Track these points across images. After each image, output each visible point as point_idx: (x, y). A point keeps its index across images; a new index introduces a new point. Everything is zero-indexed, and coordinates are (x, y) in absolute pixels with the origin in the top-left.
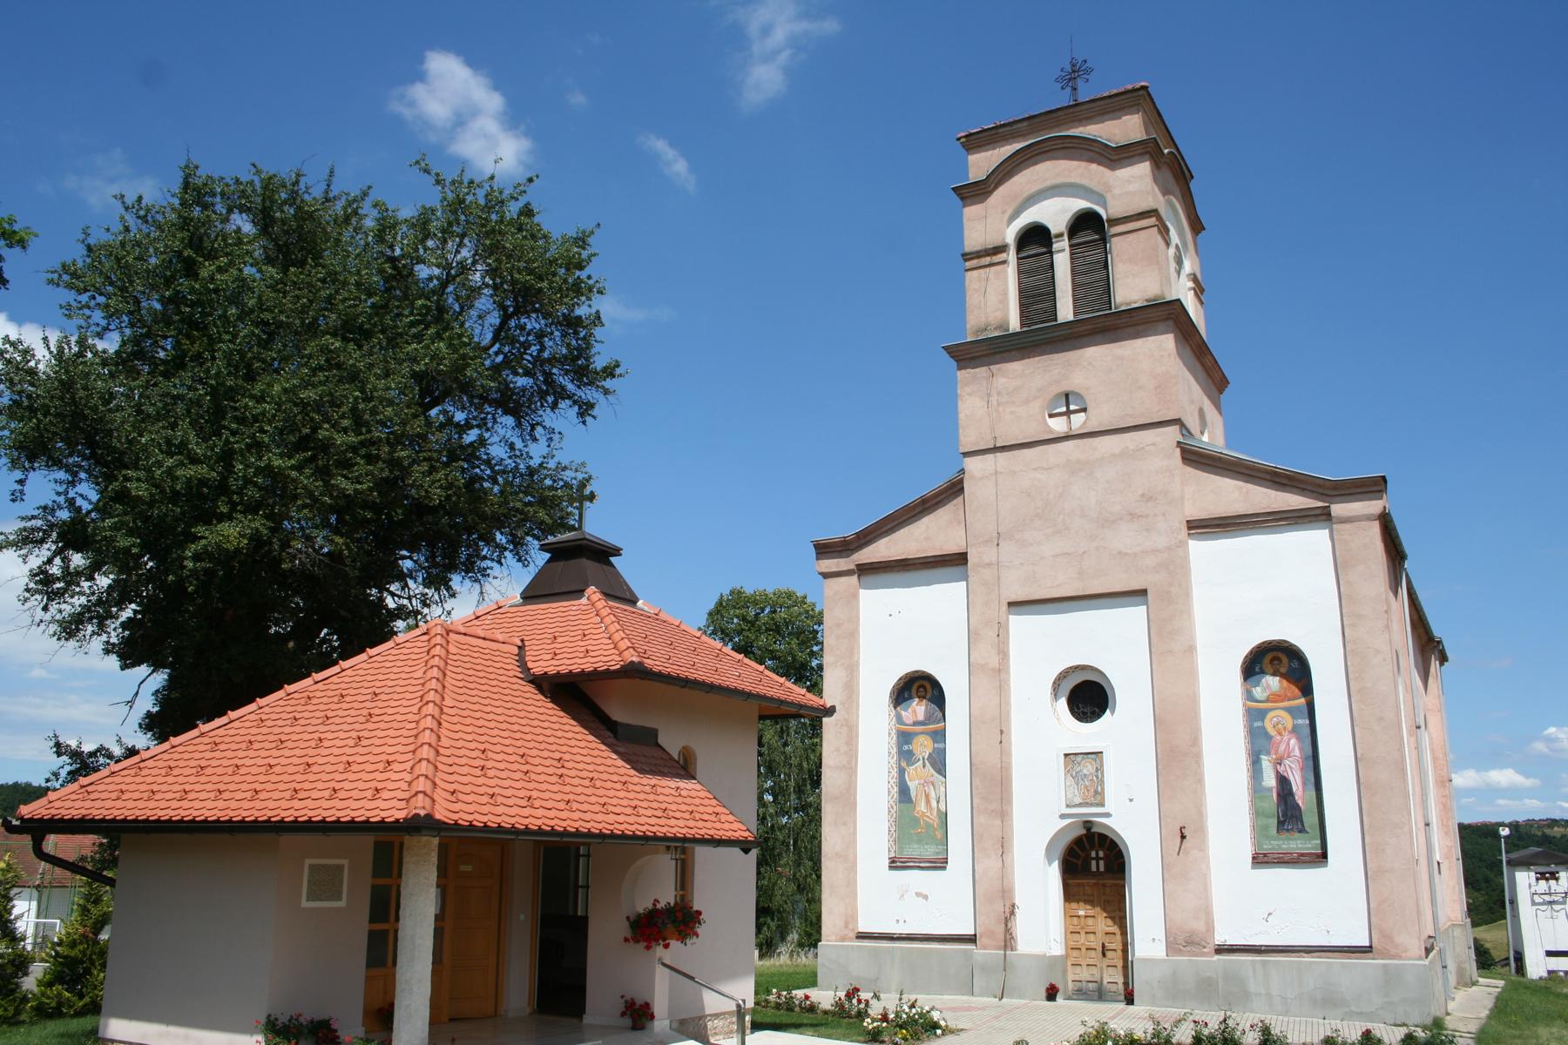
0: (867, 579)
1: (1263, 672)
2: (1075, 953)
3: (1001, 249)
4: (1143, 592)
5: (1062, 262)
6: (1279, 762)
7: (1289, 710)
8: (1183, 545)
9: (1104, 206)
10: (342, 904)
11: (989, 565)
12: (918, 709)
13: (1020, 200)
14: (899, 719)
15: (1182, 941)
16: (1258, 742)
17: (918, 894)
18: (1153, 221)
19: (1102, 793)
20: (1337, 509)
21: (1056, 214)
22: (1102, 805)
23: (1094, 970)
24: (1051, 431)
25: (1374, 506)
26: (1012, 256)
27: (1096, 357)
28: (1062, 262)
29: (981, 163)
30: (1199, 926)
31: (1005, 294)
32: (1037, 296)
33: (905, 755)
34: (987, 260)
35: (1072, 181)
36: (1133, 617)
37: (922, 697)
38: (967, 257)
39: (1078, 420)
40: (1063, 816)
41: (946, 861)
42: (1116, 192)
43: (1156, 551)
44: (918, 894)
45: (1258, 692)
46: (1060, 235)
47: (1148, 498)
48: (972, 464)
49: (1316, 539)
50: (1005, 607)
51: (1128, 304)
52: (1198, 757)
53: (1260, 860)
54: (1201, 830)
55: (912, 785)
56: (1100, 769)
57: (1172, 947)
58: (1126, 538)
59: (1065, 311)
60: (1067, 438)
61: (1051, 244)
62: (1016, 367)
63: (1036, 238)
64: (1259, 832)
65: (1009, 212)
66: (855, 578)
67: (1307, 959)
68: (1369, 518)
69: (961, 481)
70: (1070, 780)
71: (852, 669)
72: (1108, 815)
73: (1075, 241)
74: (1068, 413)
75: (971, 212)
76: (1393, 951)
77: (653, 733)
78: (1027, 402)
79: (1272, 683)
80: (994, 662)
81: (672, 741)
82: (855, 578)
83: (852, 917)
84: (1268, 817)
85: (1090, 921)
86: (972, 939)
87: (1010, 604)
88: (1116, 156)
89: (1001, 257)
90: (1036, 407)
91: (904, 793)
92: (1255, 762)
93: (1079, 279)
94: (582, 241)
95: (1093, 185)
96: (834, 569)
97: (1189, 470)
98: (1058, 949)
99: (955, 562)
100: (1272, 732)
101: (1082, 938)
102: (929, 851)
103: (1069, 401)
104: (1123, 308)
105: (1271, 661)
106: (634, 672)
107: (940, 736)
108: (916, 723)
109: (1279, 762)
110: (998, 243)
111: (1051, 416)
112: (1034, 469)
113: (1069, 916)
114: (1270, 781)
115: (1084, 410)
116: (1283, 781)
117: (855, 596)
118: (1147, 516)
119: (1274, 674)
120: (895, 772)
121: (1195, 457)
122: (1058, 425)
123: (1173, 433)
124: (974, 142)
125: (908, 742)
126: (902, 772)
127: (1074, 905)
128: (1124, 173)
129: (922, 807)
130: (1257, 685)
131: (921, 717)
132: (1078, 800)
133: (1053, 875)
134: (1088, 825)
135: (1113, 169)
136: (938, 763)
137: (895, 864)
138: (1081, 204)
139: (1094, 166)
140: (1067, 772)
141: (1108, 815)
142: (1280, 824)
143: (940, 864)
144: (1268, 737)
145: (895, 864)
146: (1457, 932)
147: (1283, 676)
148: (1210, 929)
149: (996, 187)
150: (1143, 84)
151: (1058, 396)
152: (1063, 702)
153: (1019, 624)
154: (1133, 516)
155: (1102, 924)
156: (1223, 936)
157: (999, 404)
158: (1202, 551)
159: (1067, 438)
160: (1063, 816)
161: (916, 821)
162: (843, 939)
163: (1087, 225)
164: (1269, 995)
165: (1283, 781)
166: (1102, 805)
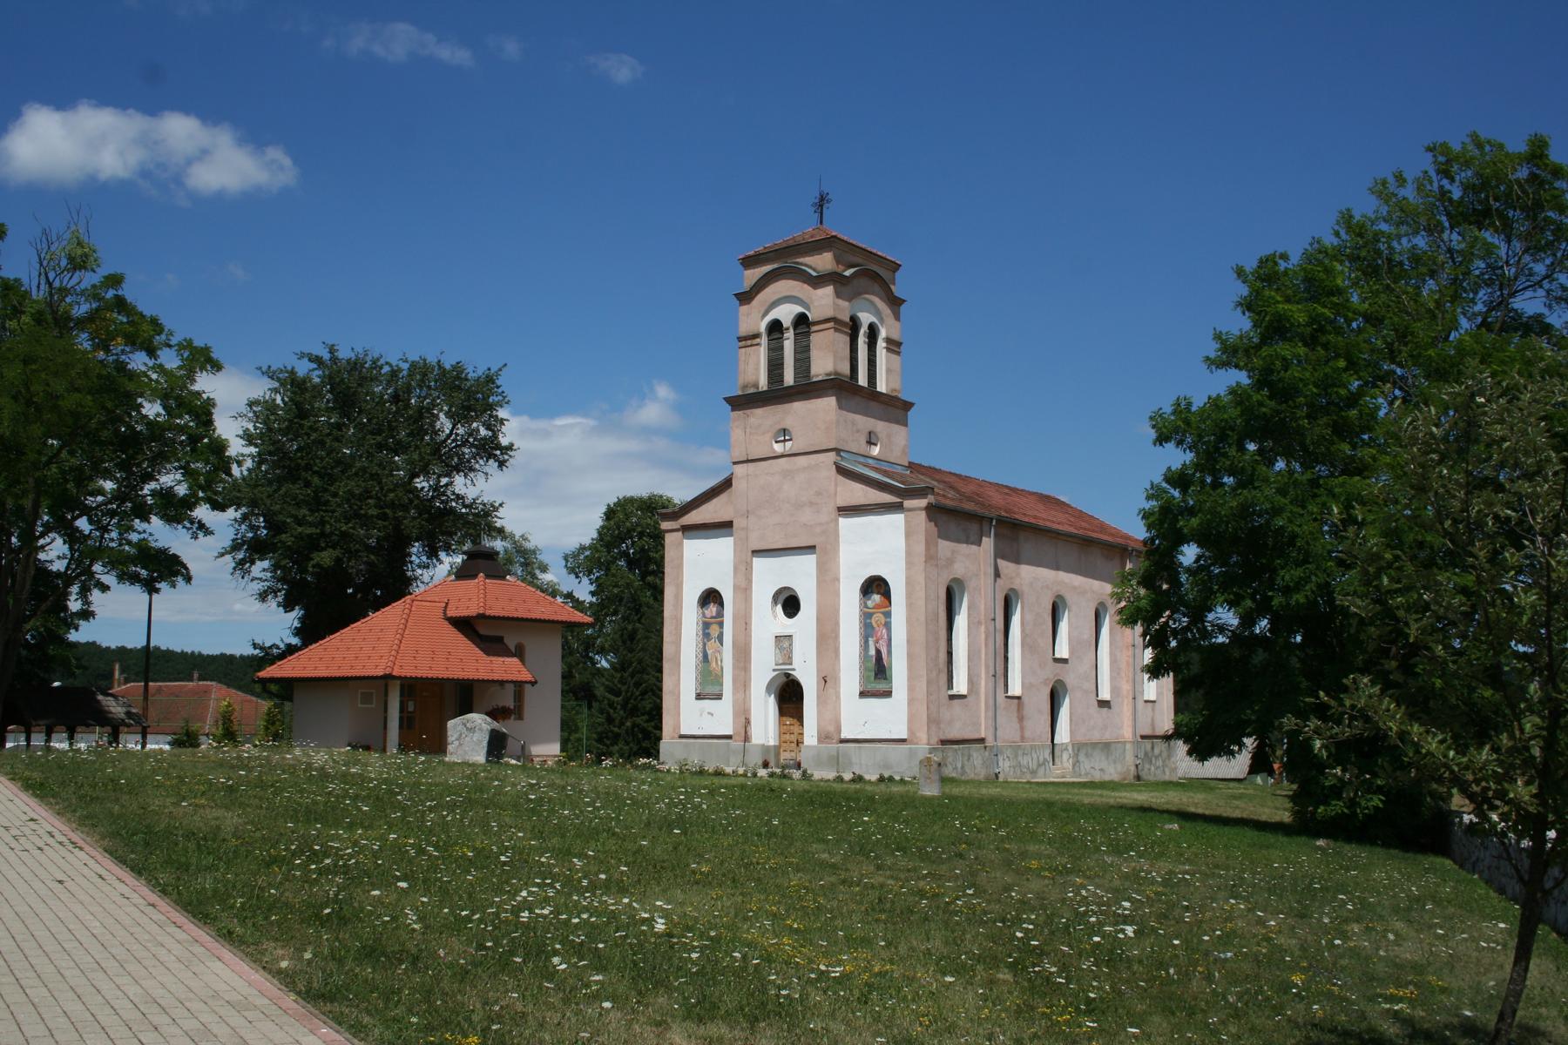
0: (686, 533)
1: (872, 592)
2: (785, 745)
3: (757, 336)
4: (814, 547)
5: (789, 345)
6: (877, 642)
7: (883, 613)
8: (837, 522)
9: (809, 311)
10: (373, 706)
11: (743, 529)
12: (712, 609)
13: (768, 304)
14: (704, 614)
15: (824, 737)
16: (867, 630)
17: (709, 713)
18: (831, 324)
19: (790, 658)
20: (908, 503)
21: (786, 313)
22: (791, 664)
23: (793, 754)
24: (774, 451)
25: (923, 503)
26: (764, 340)
27: (798, 407)
28: (789, 345)
29: (754, 274)
30: (831, 728)
31: (758, 363)
32: (775, 366)
33: (706, 636)
34: (749, 342)
35: (794, 294)
36: (808, 562)
37: (715, 603)
38: (740, 339)
39: (789, 444)
40: (774, 670)
41: (722, 695)
42: (816, 304)
43: (820, 524)
44: (709, 713)
45: (870, 603)
46: (788, 329)
47: (818, 494)
48: (739, 470)
49: (898, 519)
50: (750, 553)
51: (817, 376)
52: (837, 637)
53: (863, 694)
54: (837, 680)
55: (709, 652)
56: (791, 645)
57: (820, 741)
58: (807, 516)
59: (789, 378)
60: (782, 456)
61: (783, 334)
62: (759, 412)
63: (776, 327)
64: (864, 679)
65: (763, 310)
66: (680, 533)
67: (879, 745)
68: (920, 509)
69: (731, 479)
70: (778, 651)
71: (679, 586)
72: (794, 670)
73: (798, 331)
74: (785, 441)
75: (744, 309)
76: (915, 741)
77: (500, 640)
78: (764, 434)
79: (877, 598)
80: (743, 585)
81: (511, 643)
82: (680, 533)
83: (678, 726)
84: (870, 671)
85: (792, 727)
86: (729, 737)
87: (753, 552)
88: (817, 281)
89: (758, 340)
90: (768, 436)
91: (705, 656)
92: (866, 642)
93: (798, 356)
94: (490, 380)
95: (804, 298)
96: (670, 528)
97: (840, 478)
98: (772, 742)
99: (724, 527)
100: (874, 624)
101: (787, 737)
102: (715, 690)
103: (784, 434)
104: (815, 380)
105: (877, 586)
106: (482, 617)
107: (721, 624)
108: (712, 617)
109: (877, 642)
110: (756, 332)
111: (776, 442)
112: (767, 474)
113: (781, 724)
114: (872, 652)
115: (790, 440)
116: (878, 652)
117: (681, 545)
118: (817, 504)
119: (878, 593)
120: (701, 646)
121: (842, 471)
122: (778, 448)
123: (832, 455)
124: (749, 262)
125: (708, 628)
126: (704, 645)
127: (784, 718)
128: (820, 292)
129: (714, 665)
130: (869, 599)
131: (714, 614)
132: (781, 662)
133: (772, 701)
134: (788, 675)
135: (815, 288)
136: (720, 638)
137: (699, 697)
138: (800, 309)
139: (806, 286)
140: (776, 646)
141: (794, 670)
142: (876, 675)
143: (719, 697)
144: (873, 628)
145: (699, 697)
146: (1128, 746)
147: (882, 595)
148: (839, 732)
149: (756, 295)
150: (834, 234)
151: (780, 430)
152: (779, 608)
153: (759, 563)
154: (811, 504)
155: (796, 729)
156: (844, 735)
157: (750, 433)
158: (845, 523)
159: (782, 456)
160: (774, 670)
161: (710, 672)
162: (673, 738)
163: (801, 321)
164: (861, 764)
165: (878, 652)
166: (791, 664)
